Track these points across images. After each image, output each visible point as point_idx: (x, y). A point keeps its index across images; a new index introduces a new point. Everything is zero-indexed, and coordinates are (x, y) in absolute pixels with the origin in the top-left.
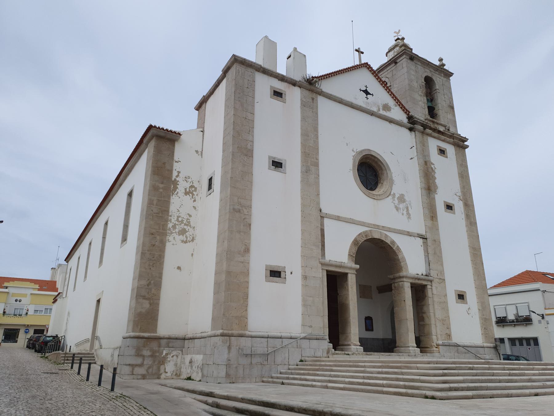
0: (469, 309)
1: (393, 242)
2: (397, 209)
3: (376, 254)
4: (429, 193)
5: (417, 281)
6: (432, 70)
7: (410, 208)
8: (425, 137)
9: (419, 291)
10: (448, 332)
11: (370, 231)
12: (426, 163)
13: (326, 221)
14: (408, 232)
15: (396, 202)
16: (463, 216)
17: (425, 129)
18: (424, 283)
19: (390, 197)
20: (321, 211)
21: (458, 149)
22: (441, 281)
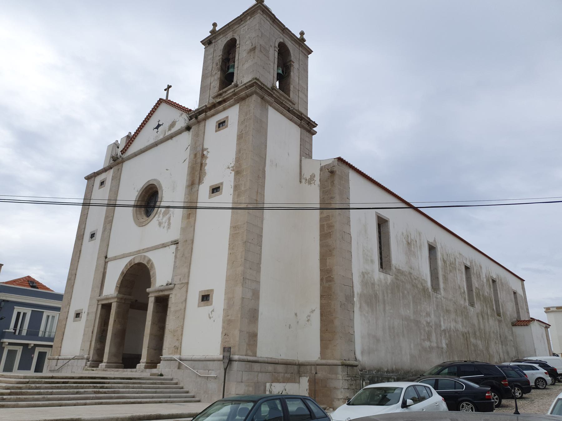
0: (213, 311)
1: (149, 260)
2: (160, 224)
3: (137, 276)
4: (192, 189)
5: (161, 294)
6: (236, 27)
7: (172, 218)
8: (202, 124)
9: (163, 302)
10: (177, 344)
11: (134, 259)
12: (195, 155)
13: (110, 265)
14: (163, 244)
15: (161, 216)
16: (232, 190)
17: (196, 118)
18: (166, 293)
19: (157, 216)
20: (106, 257)
21: (243, 102)
22: (182, 285)
